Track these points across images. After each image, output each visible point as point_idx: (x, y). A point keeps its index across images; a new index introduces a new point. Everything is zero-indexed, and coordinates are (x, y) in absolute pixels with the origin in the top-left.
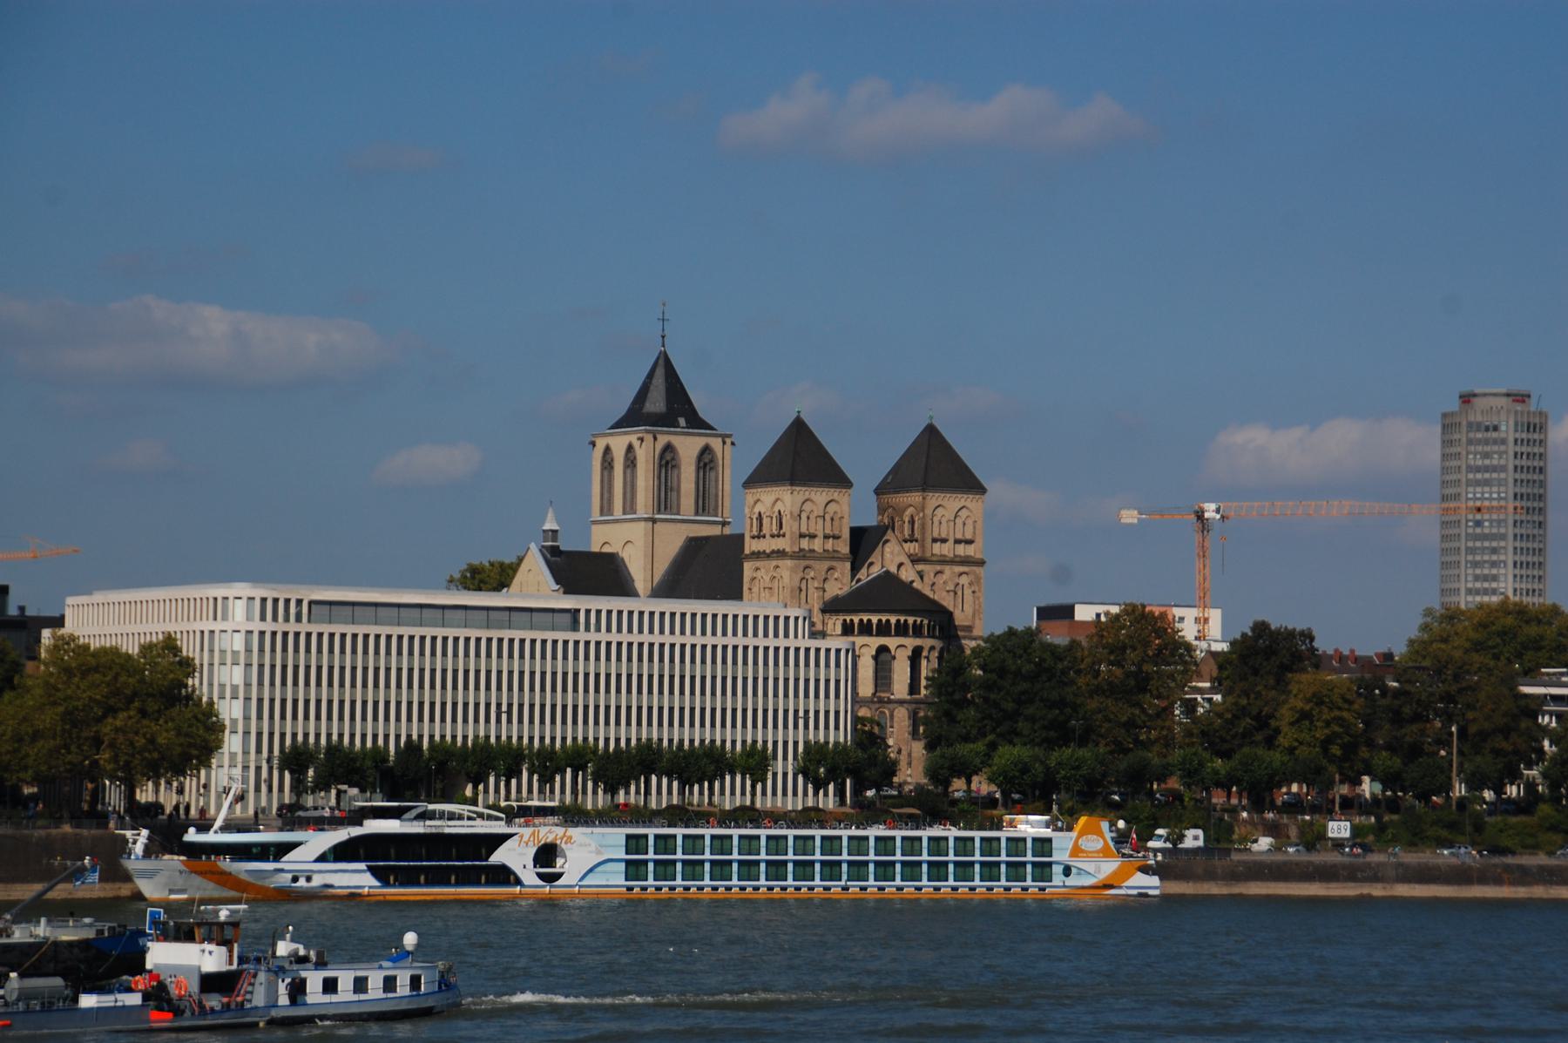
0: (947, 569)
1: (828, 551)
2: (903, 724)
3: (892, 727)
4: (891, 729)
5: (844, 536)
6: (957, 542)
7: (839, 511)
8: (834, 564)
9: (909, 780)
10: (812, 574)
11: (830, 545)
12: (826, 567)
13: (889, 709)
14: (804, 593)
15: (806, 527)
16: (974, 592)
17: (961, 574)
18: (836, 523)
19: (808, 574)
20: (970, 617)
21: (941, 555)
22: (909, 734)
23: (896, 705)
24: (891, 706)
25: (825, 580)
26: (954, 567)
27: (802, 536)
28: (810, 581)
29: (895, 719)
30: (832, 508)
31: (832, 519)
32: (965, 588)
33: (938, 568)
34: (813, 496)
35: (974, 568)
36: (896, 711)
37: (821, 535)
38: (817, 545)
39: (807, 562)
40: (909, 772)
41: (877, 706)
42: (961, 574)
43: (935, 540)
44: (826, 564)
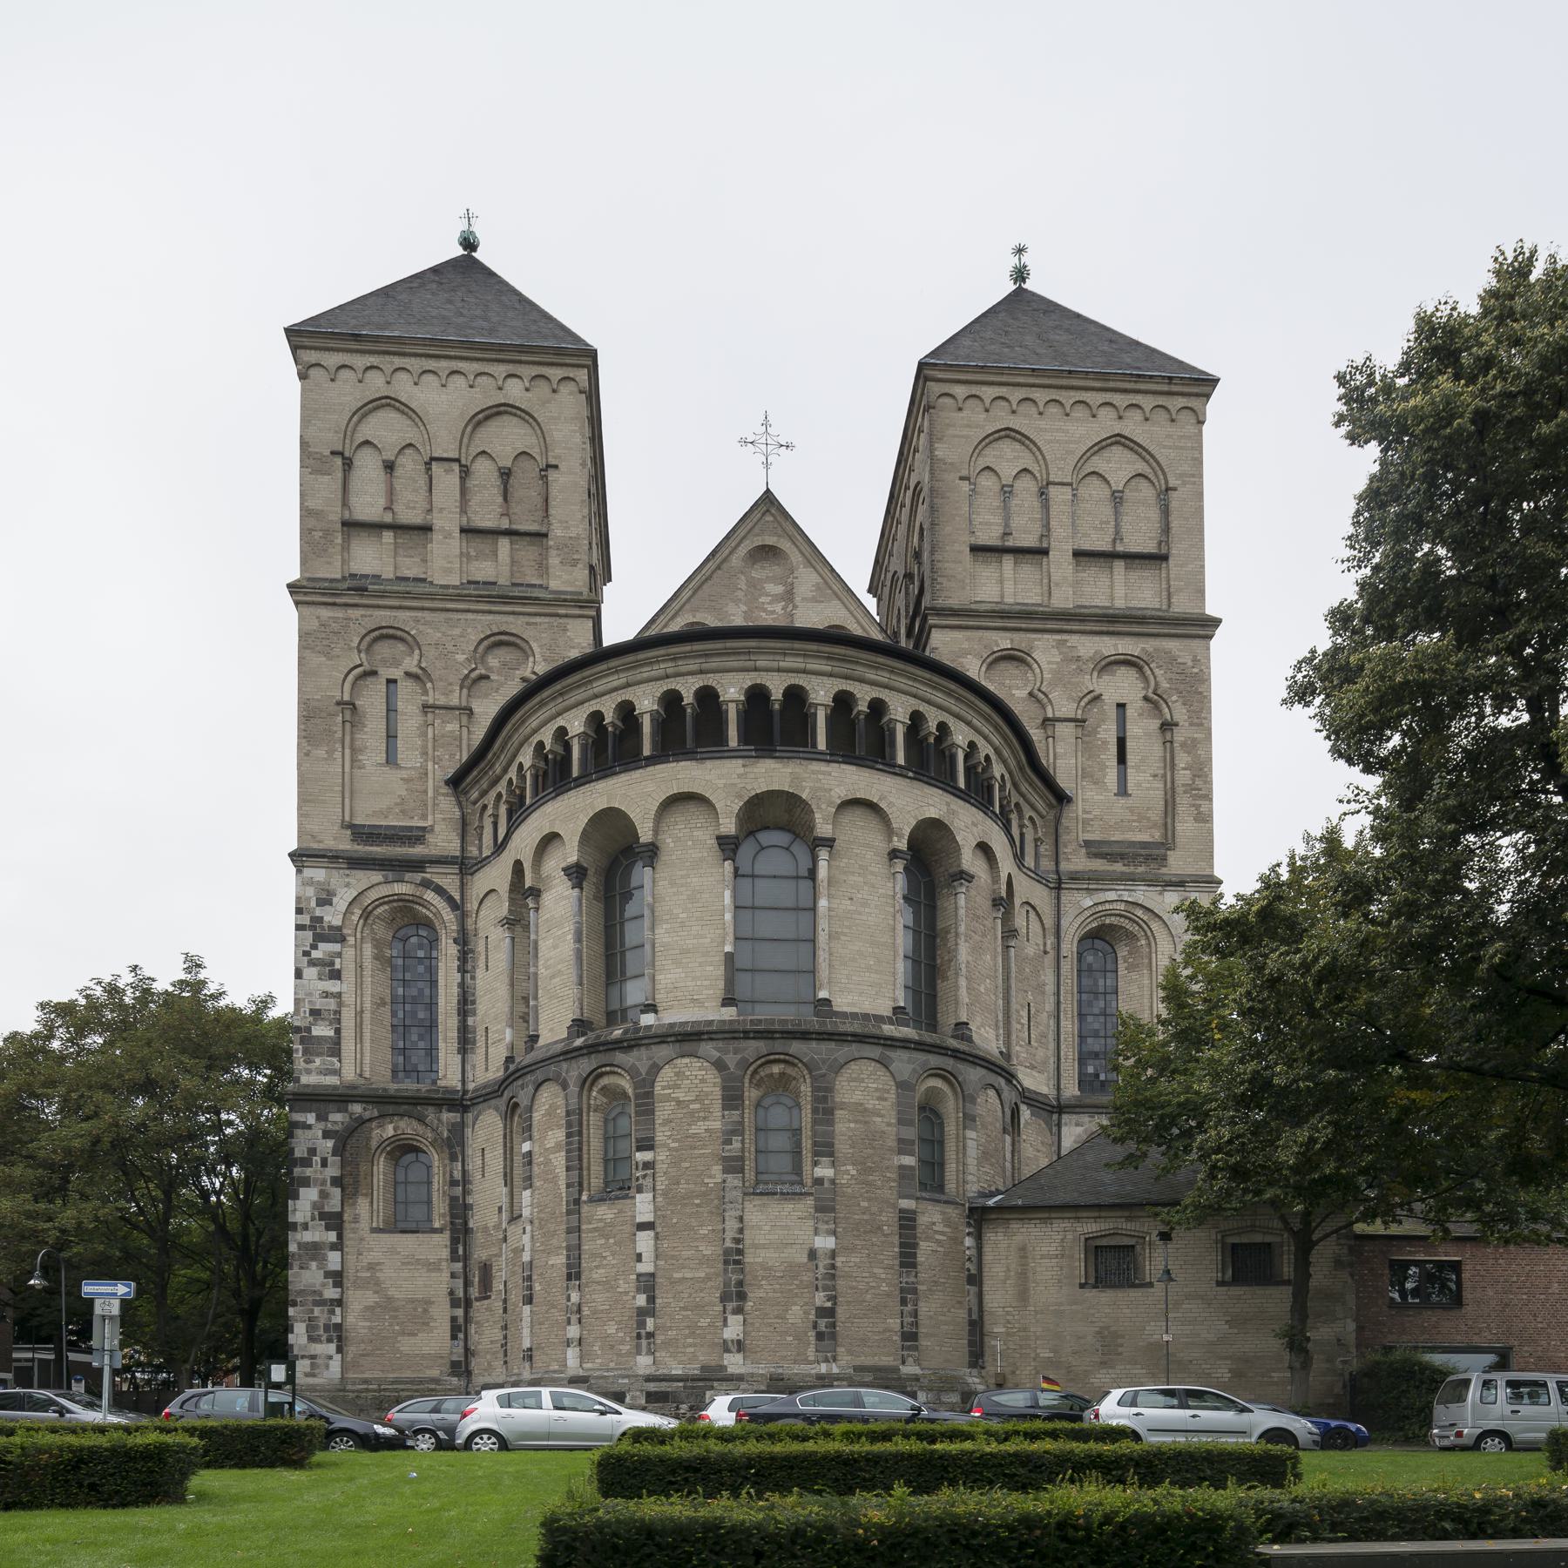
2: (699, 1128)
3: (647, 1144)
4: (641, 1156)
5: (557, 532)
7: (535, 452)
8: (515, 625)
9: (734, 1363)
10: (410, 664)
11: (497, 565)
12: (474, 637)
13: (633, 1072)
15: (382, 502)
16: (1167, 726)
17: (1108, 665)
18: (526, 489)
20: (1156, 814)
22: (733, 1165)
23: (663, 1051)
24: (638, 1059)
26: (1073, 640)
27: (352, 526)
28: (405, 688)
29: (663, 1111)
30: (506, 439)
31: (506, 475)
32: (1130, 712)
33: (1004, 641)
36: (667, 1074)
37: (447, 521)
39: (382, 617)
40: (733, 1330)
41: (585, 1065)
44: (476, 626)
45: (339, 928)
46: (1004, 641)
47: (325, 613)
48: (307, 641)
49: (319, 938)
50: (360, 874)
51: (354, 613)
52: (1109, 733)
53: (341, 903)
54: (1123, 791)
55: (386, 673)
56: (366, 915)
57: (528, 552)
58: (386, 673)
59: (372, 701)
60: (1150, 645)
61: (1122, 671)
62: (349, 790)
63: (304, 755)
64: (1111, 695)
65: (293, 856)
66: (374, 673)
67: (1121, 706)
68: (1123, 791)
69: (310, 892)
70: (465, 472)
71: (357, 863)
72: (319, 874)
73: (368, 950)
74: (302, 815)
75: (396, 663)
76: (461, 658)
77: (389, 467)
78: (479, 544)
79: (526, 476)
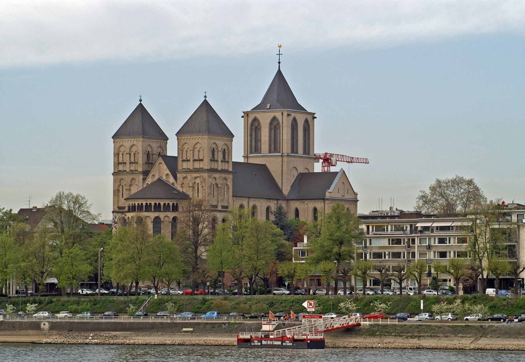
0: (189, 176)
1: (133, 170)
5: (139, 163)
6: (195, 160)
14: (121, 192)
17: (196, 178)
19: (123, 183)
21: (188, 169)
25: (130, 186)
28: (124, 186)
31: (134, 154)
32: (199, 184)
33: (184, 175)
34: (124, 144)
35: (203, 174)
37: (128, 162)
38: (127, 168)
42: (196, 178)
43: (183, 161)
44: (130, 177)
45: (117, 222)
46: (184, 175)
47: (116, 177)
48: (115, 181)
49: (115, 223)
50: (119, 214)
51: (119, 177)
52: (196, 188)
53: (117, 218)
54: (198, 196)
55: (122, 184)
56: (120, 219)
57: (136, 165)
58: (122, 184)
59: (121, 189)
60: (200, 174)
61: (198, 178)
62: (118, 202)
63: (114, 197)
64: (197, 182)
65: (112, 212)
66: (121, 185)
67: (198, 183)
68: (198, 196)
69: (114, 217)
70: (130, 154)
71: (118, 212)
72: (115, 214)
73: (120, 224)
74: (113, 206)
75: (123, 183)
76: (129, 182)
77: (123, 154)
78: (131, 165)
79: (137, 153)
